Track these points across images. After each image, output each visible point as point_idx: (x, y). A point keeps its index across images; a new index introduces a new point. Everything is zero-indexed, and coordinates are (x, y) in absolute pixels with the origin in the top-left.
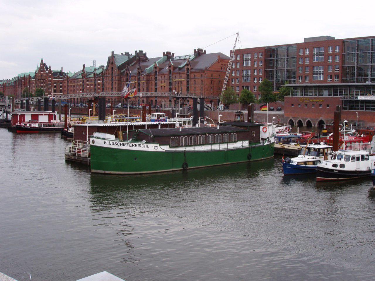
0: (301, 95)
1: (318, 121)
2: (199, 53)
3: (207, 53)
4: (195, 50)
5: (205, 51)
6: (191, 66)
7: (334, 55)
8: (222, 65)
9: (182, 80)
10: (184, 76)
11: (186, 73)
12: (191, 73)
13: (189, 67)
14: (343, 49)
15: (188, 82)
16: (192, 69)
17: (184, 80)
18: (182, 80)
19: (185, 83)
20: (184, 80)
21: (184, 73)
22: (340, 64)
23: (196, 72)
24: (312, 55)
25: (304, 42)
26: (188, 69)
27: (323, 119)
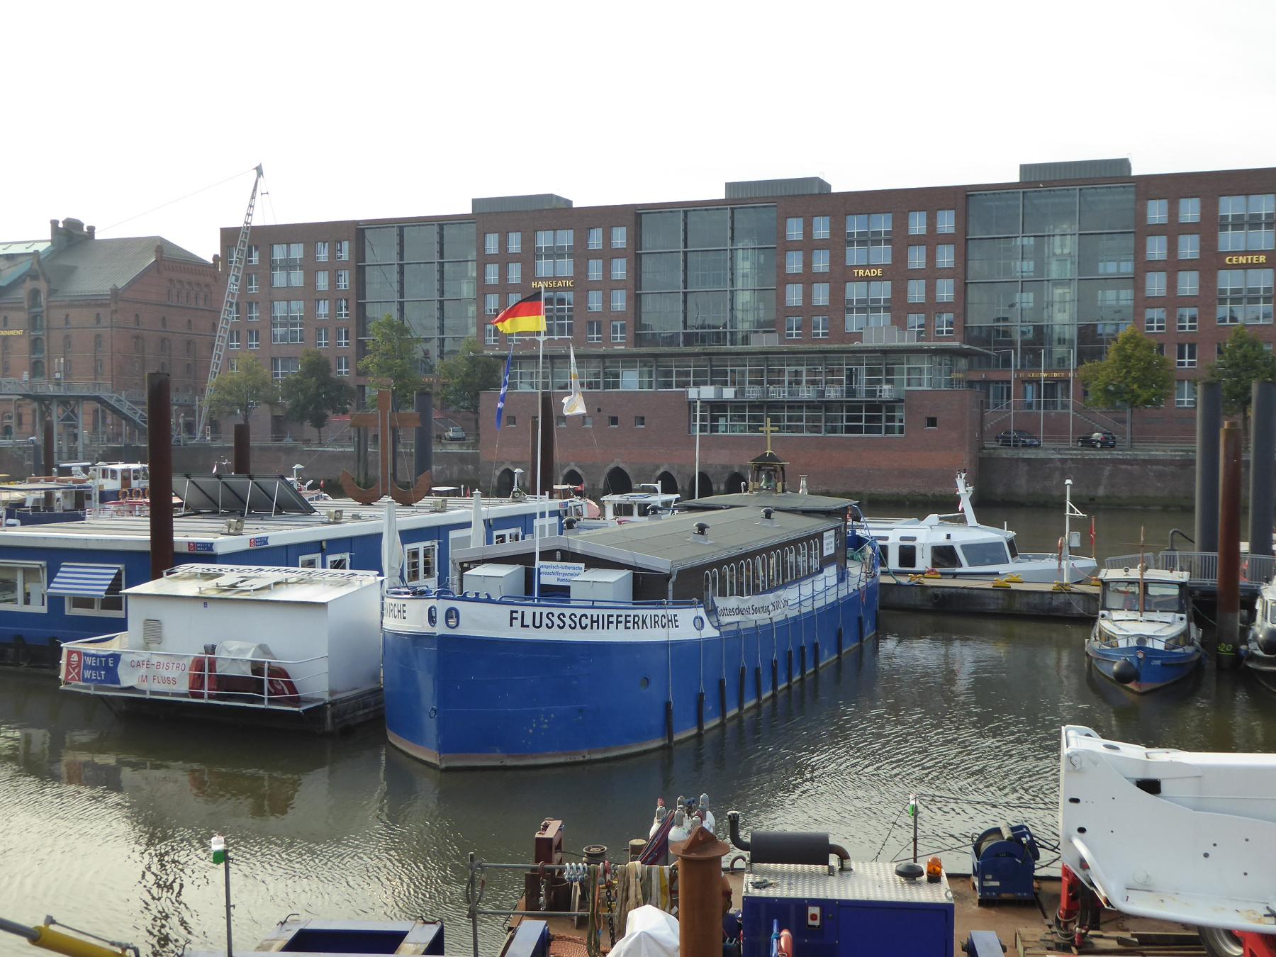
0: (646, 385)
1: (607, 470)
2: (71, 236)
3: (98, 236)
4: (54, 223)
5: (91, 229)
6: (48, 281)
7: (607, 254)
8: (171, 280)
9: (13, 333)
10: (22, 316)
11: (26, 305)
12: (48, 308)
13: (42, 285)
14: (636, 239)
15: (36, 345)
16: (52, 292)
17: (19, 332)
18: (13, 333)
19: (24, 345)
20: (19, 332)
21: (20, 309)
22: (631, 284)
23: (72, 305)
24: (530, 256)
25: (470, 212)
26: (35, 294)
27: (621, 466)
